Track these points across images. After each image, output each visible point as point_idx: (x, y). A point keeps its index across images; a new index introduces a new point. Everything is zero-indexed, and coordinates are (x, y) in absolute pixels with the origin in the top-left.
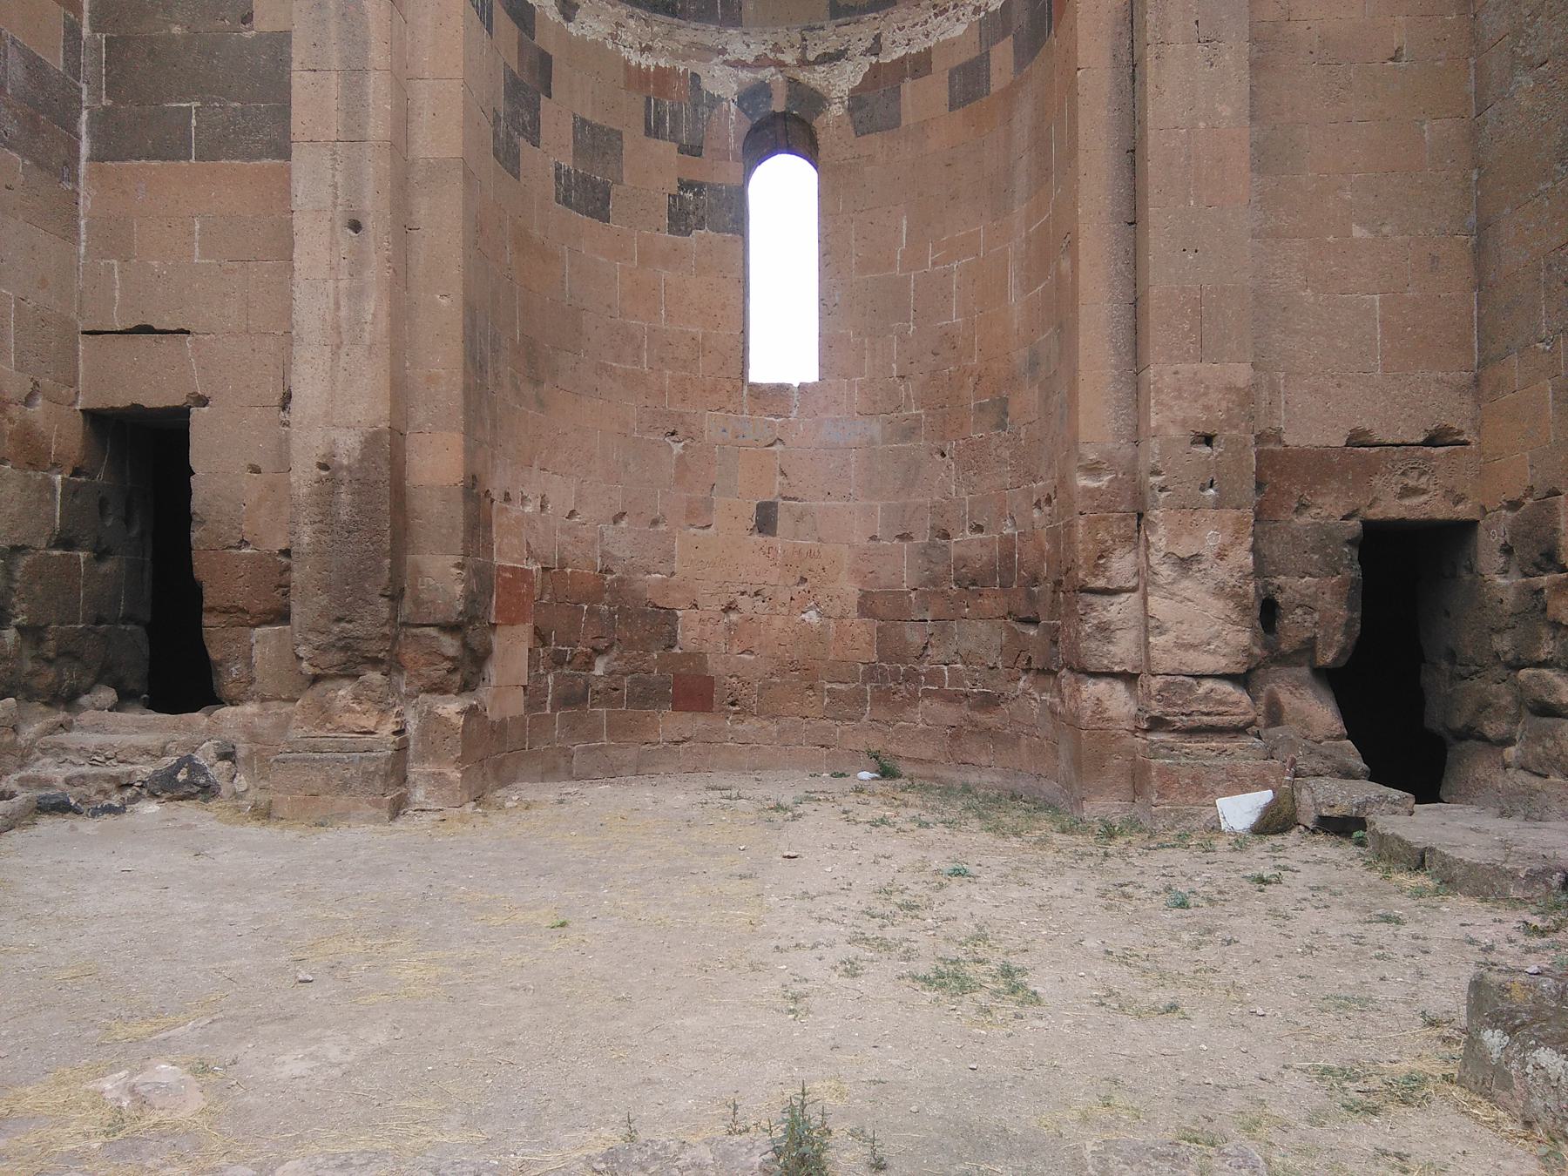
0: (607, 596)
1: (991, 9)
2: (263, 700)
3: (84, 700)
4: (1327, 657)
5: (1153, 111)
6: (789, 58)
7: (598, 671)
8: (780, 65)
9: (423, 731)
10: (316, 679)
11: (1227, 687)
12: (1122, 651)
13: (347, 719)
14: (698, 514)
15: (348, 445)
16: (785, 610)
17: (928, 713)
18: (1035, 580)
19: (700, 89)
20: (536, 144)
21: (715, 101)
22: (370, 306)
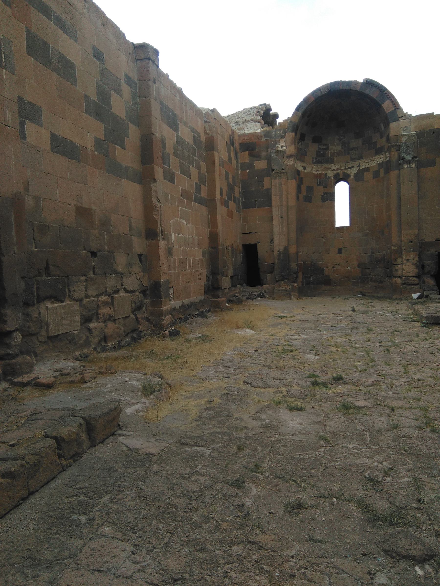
2: (269, 284)
4: (432, 273)
10: (277, 281)
12: (399, 273)
13: (283, 286)
15: (282, 248)
16: (344, 267)
20: (301, 193)
21: (329, 177)
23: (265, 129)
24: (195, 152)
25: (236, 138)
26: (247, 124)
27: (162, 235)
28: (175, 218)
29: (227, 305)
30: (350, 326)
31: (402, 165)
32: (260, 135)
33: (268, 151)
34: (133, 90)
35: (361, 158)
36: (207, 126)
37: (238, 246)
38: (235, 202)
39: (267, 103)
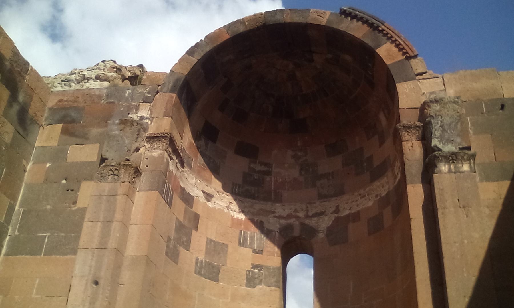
1: (383, 195)
6: (301, 215)
8: (298, 218)
19: (263, 227)
32: (97, 93)
35: (340, 192)
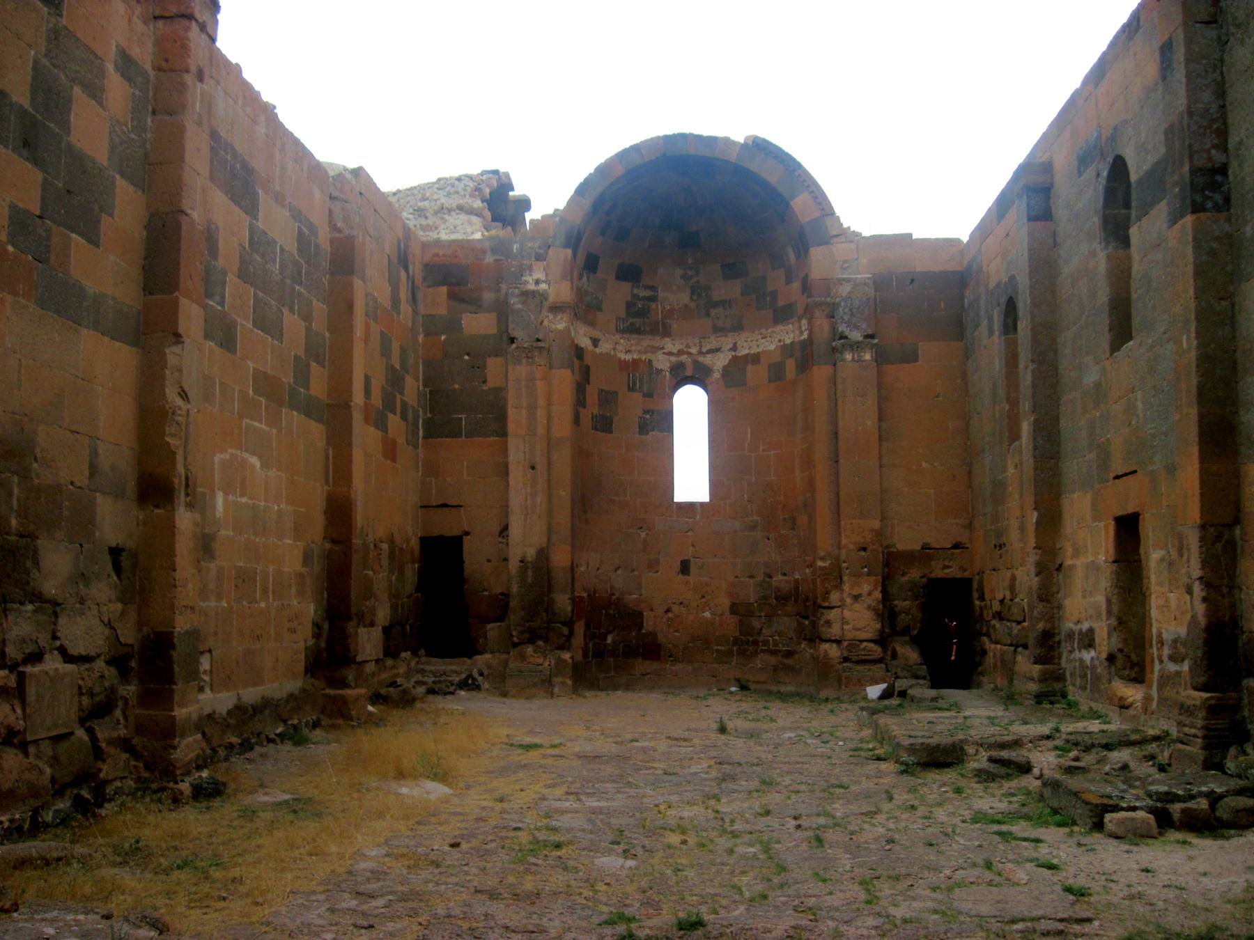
0: (613, 607)
2: (492, 652)
3: (420, 653)
5: (840, 424)
6: (694, 350)
7: (609, 639)
8: (690, 354)
9: (557, 664)
10: (515, 645)
11: (871, 645)
12: (835, 631)
13: (531, 659)
14: (652, 565)
15: (531, 553)
17: (762, 660)
18: (807, 600)
20: (584, 407)
21: (659, 371)
22: (539, 499)
23: (494, 232)
24: (299, 273)
25: (415, 250)
26: (446, 217)
27: (187, 495)
28: (230, 450)
29: (370, 708)
30: (714, 774)
31: (841, 352)
33: (498, 291)
34: (137, 93)
35: (738, 328)
36: (337, 208)
37: (408, 541)
38: (404, 416)
39: (502, 170)
